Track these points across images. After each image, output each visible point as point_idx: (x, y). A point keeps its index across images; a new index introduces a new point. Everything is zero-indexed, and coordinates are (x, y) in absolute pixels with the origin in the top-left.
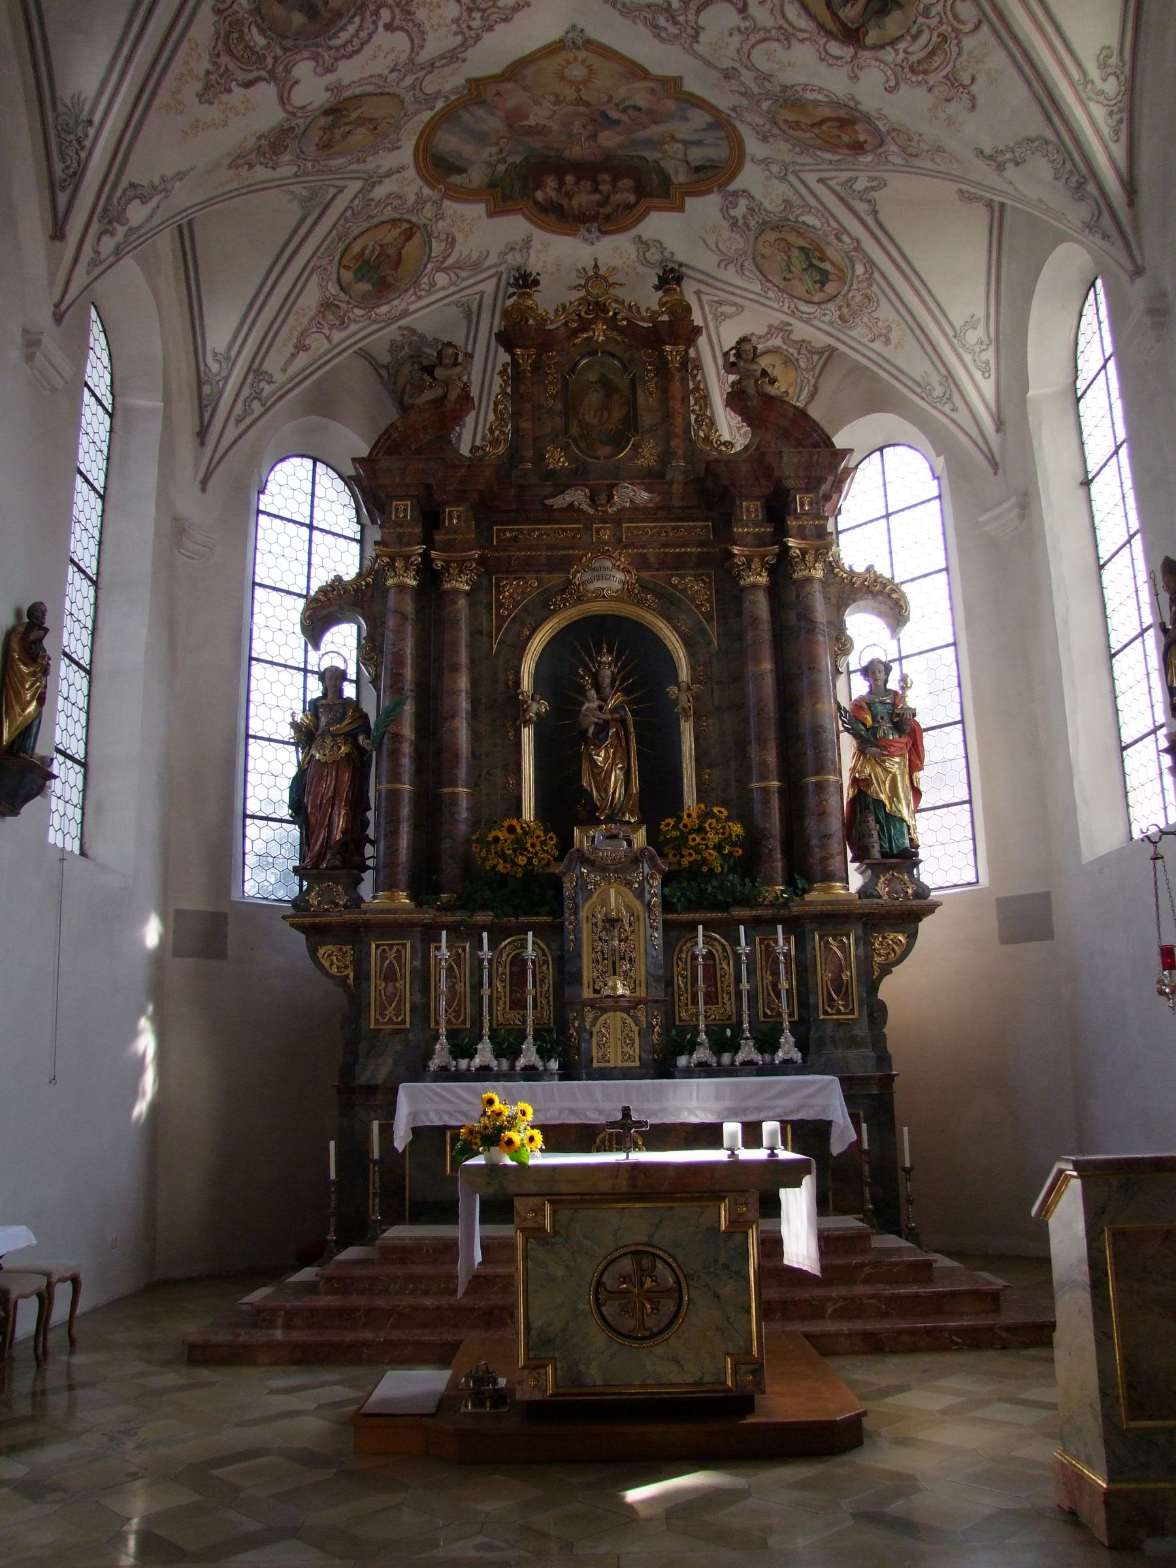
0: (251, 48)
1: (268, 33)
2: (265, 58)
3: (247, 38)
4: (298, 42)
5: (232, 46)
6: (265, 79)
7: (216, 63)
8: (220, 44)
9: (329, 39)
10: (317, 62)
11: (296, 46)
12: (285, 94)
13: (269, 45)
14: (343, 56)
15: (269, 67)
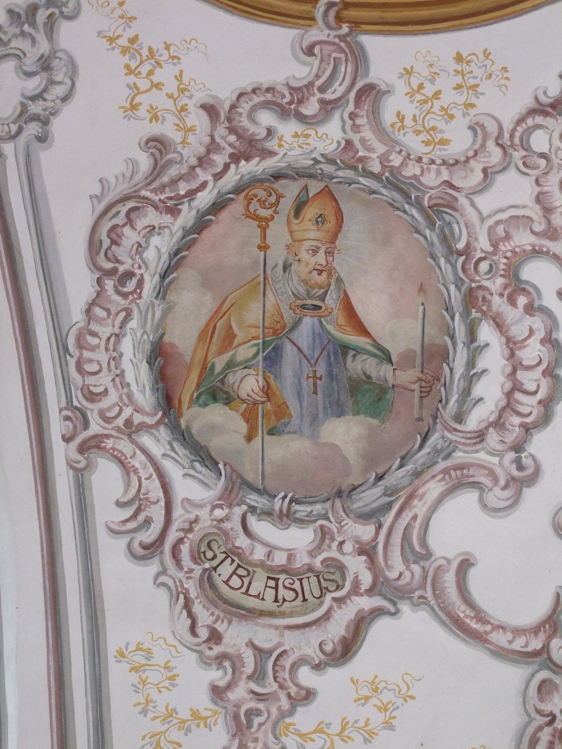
0: (284, 570)
1: (302, 510)
2: (341, 568)
3: (259, 554)
4: (390, 480)
5: (237, 597)
6: (378, 612)
7: (222, 657)
8: (198, 608)
9: (459, 418)
10: (476, 485)
11: (391, 492)
12: (462, 611)
13: (324, 533)
14: (527, 429)
15: (366, 579)
